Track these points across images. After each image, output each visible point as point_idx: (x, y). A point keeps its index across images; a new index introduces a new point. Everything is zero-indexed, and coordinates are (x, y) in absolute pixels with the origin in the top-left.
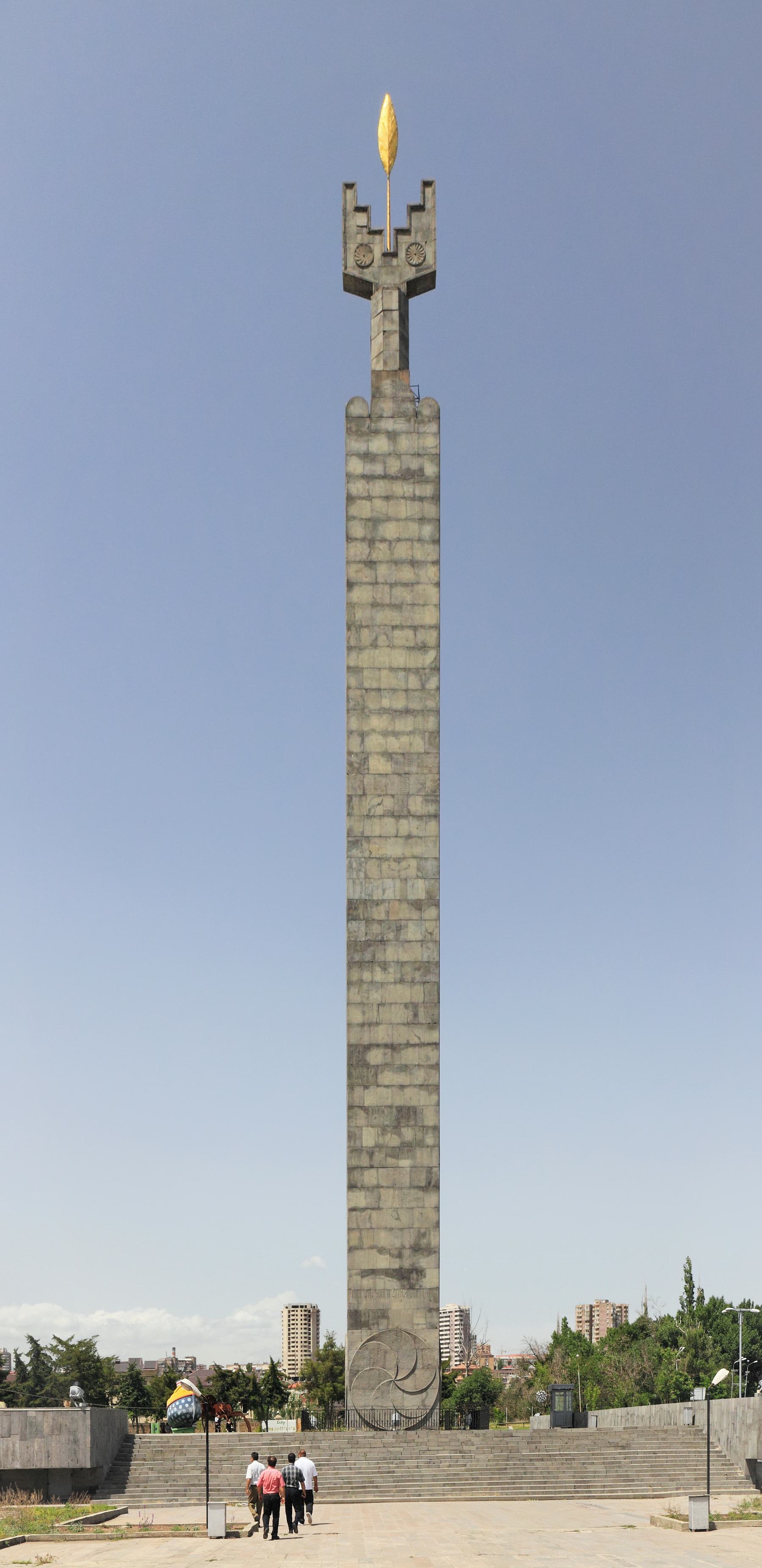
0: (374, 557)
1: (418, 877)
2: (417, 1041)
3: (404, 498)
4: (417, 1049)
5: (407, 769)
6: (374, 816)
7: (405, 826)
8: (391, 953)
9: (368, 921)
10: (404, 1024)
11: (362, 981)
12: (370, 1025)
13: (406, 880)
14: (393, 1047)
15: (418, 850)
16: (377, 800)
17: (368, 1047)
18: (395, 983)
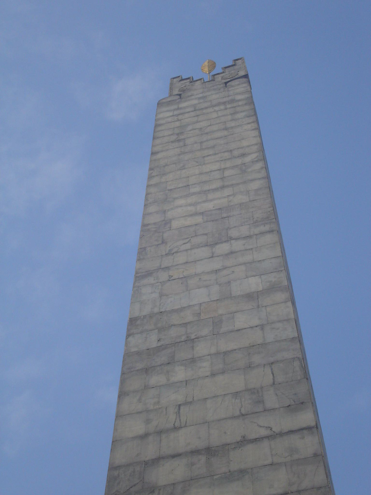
0: (182, 137)
1: (247, 277)
2: (264, 432)
3: (215, 111)
4: (266, 443)
5: (225, 215)
6: (177, 252)
7: (224, 248)
8: (202, 349)
9: (161, 330)
10: (233, 417)
11: (146, 387)
12: (160, 433)
13: (229, 282)
14: (209, 451)
15: (248, 258)
16: (181, 242)
17: (157, 461)
18: (213, 375)
